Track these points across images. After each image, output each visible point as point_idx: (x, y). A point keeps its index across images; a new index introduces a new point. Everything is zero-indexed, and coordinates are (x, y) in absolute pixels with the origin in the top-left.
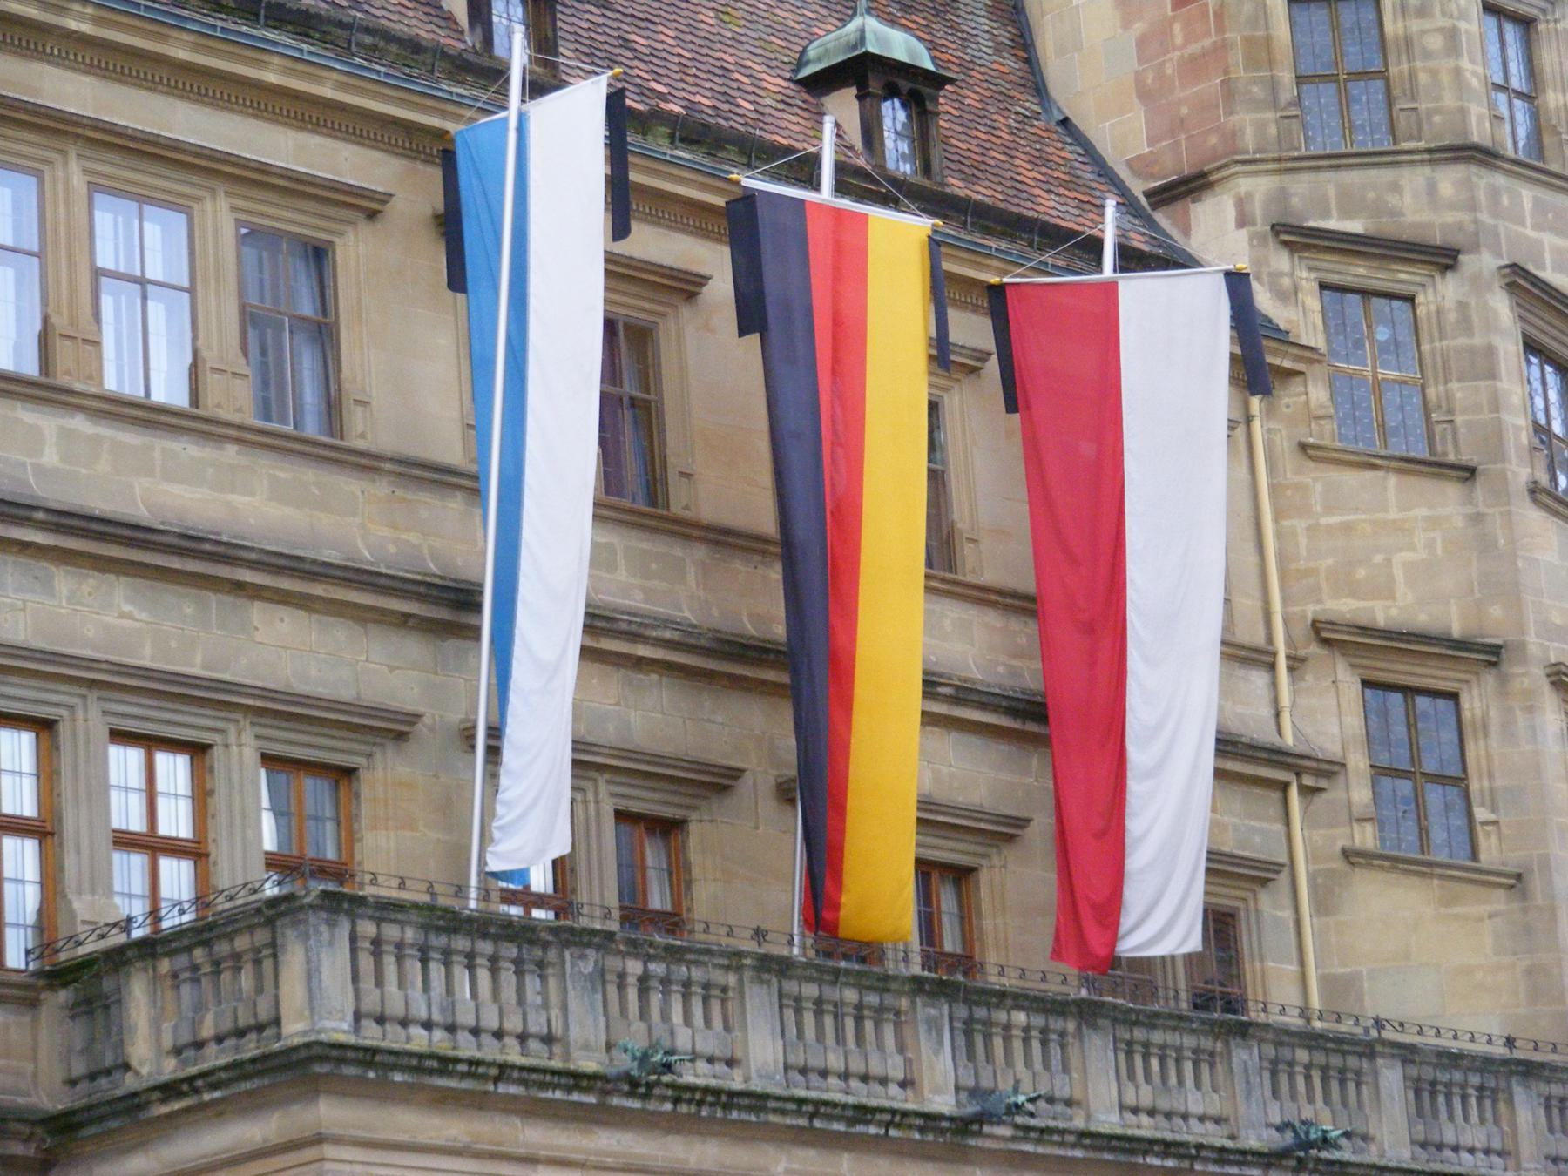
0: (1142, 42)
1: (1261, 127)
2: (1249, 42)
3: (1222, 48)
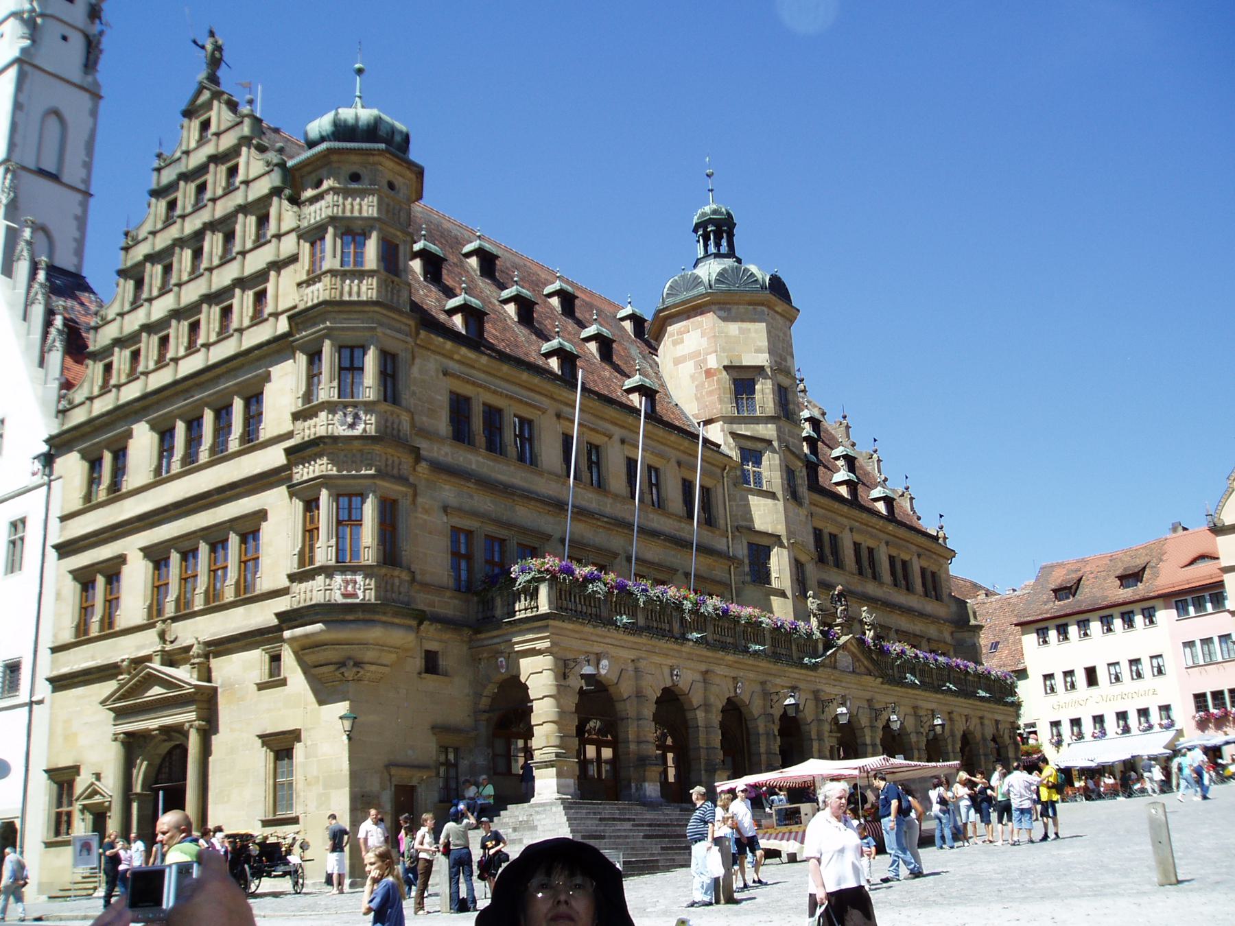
1: (727, 408)
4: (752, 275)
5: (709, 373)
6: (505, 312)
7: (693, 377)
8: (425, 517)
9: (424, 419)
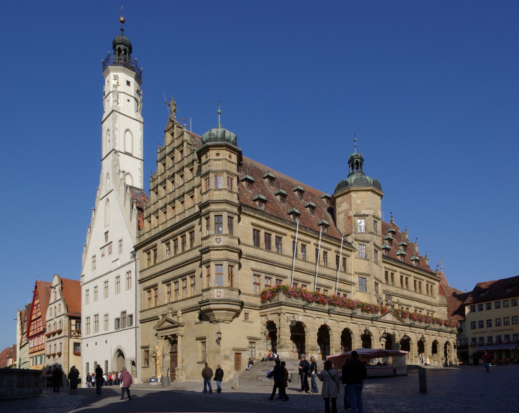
0: (345, 223)
1: (354, 230)
2: (354, 223)
3: (351, 224)
4: (367, 180)
5: (349, 218)
6: (276, 199)
7: (344, 219)
8: (245, 271)
9: (244, 239)
